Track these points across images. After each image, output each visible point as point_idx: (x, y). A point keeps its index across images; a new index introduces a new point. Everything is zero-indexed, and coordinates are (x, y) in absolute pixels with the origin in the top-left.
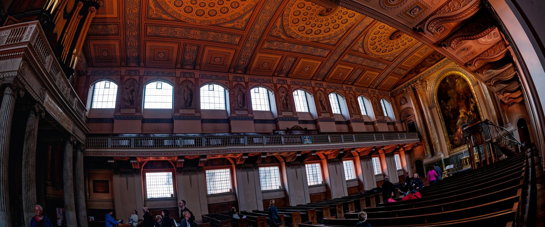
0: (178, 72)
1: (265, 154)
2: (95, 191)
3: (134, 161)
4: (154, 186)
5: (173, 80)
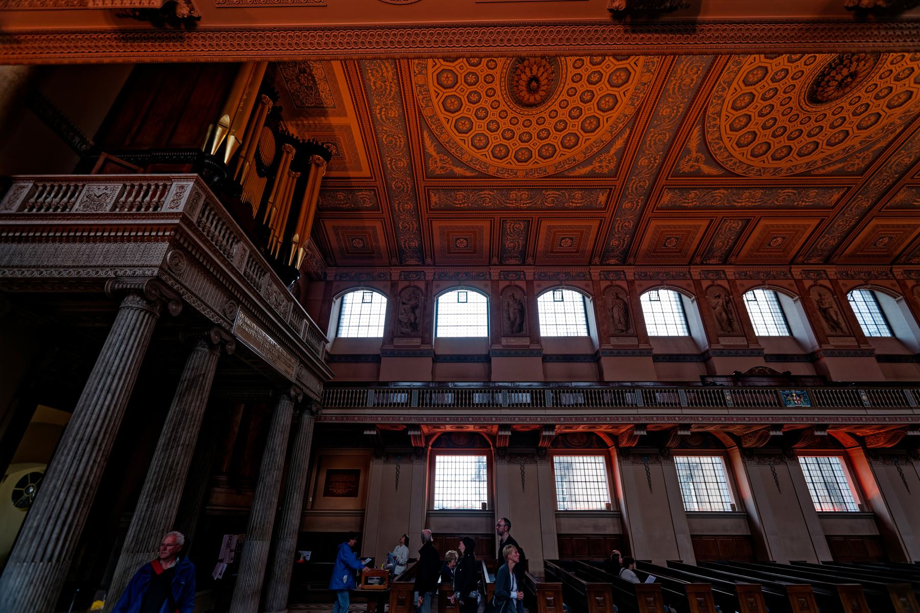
0: (495, 272)
1: (687, 427)
2: (328, 493)
3: (416, 433)
4: (449, 479)
5: (486, 286)
